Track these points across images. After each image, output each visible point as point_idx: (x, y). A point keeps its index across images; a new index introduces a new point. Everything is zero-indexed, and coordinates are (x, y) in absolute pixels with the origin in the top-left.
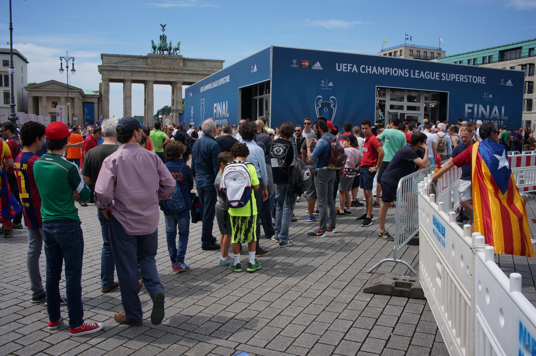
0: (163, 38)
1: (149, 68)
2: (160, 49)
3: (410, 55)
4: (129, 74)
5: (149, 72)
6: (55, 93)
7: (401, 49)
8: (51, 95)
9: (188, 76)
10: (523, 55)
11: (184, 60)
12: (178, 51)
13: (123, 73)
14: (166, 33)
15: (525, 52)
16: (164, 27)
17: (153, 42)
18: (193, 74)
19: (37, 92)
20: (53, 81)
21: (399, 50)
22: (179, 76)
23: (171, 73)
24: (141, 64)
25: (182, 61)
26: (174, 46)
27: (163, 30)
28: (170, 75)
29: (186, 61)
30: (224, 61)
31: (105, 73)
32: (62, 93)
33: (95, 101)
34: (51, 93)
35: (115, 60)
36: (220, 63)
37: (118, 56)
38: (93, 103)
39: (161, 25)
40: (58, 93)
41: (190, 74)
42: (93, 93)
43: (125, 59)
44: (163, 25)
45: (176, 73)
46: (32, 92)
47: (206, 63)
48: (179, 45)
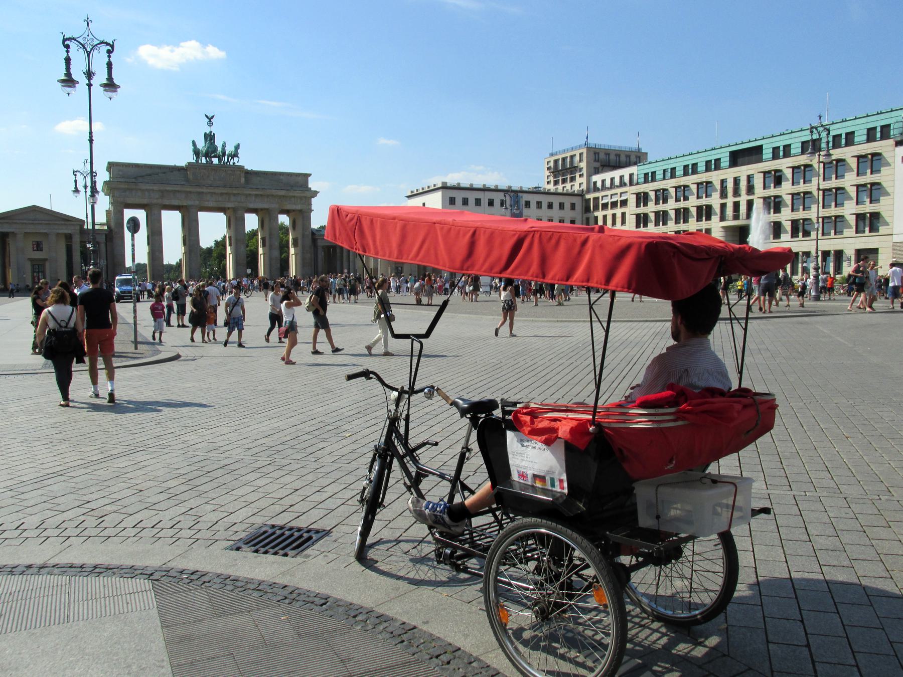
2: (207, 155)
3: (595, 161)
5: (190, 192)
7: (581, 151)
8: (31, 229)
10: (764, 157)
12: (236, 159)
14: (214, 130)
15: (767, 153)
16: (210, 119)
17: (194, 143)
20: (34, 206)
21: (577, 153)
25: (243, 175)
26: (229, 149)
27: (210, 123)
30: (310, 175)
39: (207, 116)
41: (256, 195)
44: (210, 115)
45: (234, 195)
47: (281, 177)
48: (237, 147)
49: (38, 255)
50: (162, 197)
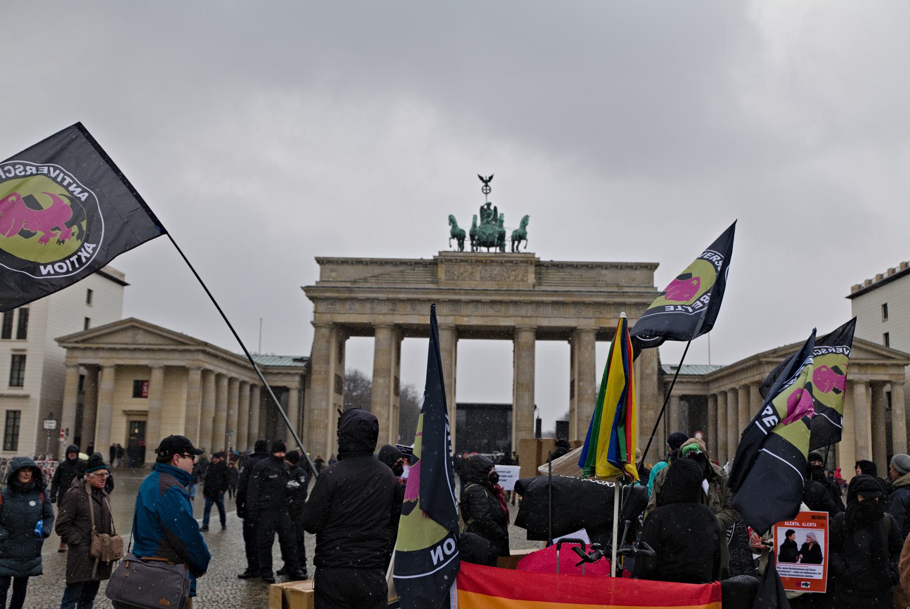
0: (488, 213)
1: (440, 291)
4: (384, 308)
6: (138, 355)
9: (549, 310)
11: (539, 264)
13: (368, 306)
14: (495, 199)
16: (486, 182)
17: (452, 221)
18: (563, 304)
19: (89, 354)
20: (132, 320)
22: (523, 311)
23: (501, 302)
24: (420, 282)
25: (532, 269)
27: (487, 189)
28: (498, 307)
29: (544, 270)
31: (323, 307)
33: (293, 383)
35: (352, 272)
36: (645, 271)
37: (359, 262)
38: (286, 390)
39: (481, 178)
40: (145, 355)
41: (555, 303)
42: (290, 363)
43: (378, 270)
44: (486, 176)
45: (515, 303)
46: (77, 353)
47: (604, 272)
48: (524, 222)
49: (139, 404)
50: (393, 311)
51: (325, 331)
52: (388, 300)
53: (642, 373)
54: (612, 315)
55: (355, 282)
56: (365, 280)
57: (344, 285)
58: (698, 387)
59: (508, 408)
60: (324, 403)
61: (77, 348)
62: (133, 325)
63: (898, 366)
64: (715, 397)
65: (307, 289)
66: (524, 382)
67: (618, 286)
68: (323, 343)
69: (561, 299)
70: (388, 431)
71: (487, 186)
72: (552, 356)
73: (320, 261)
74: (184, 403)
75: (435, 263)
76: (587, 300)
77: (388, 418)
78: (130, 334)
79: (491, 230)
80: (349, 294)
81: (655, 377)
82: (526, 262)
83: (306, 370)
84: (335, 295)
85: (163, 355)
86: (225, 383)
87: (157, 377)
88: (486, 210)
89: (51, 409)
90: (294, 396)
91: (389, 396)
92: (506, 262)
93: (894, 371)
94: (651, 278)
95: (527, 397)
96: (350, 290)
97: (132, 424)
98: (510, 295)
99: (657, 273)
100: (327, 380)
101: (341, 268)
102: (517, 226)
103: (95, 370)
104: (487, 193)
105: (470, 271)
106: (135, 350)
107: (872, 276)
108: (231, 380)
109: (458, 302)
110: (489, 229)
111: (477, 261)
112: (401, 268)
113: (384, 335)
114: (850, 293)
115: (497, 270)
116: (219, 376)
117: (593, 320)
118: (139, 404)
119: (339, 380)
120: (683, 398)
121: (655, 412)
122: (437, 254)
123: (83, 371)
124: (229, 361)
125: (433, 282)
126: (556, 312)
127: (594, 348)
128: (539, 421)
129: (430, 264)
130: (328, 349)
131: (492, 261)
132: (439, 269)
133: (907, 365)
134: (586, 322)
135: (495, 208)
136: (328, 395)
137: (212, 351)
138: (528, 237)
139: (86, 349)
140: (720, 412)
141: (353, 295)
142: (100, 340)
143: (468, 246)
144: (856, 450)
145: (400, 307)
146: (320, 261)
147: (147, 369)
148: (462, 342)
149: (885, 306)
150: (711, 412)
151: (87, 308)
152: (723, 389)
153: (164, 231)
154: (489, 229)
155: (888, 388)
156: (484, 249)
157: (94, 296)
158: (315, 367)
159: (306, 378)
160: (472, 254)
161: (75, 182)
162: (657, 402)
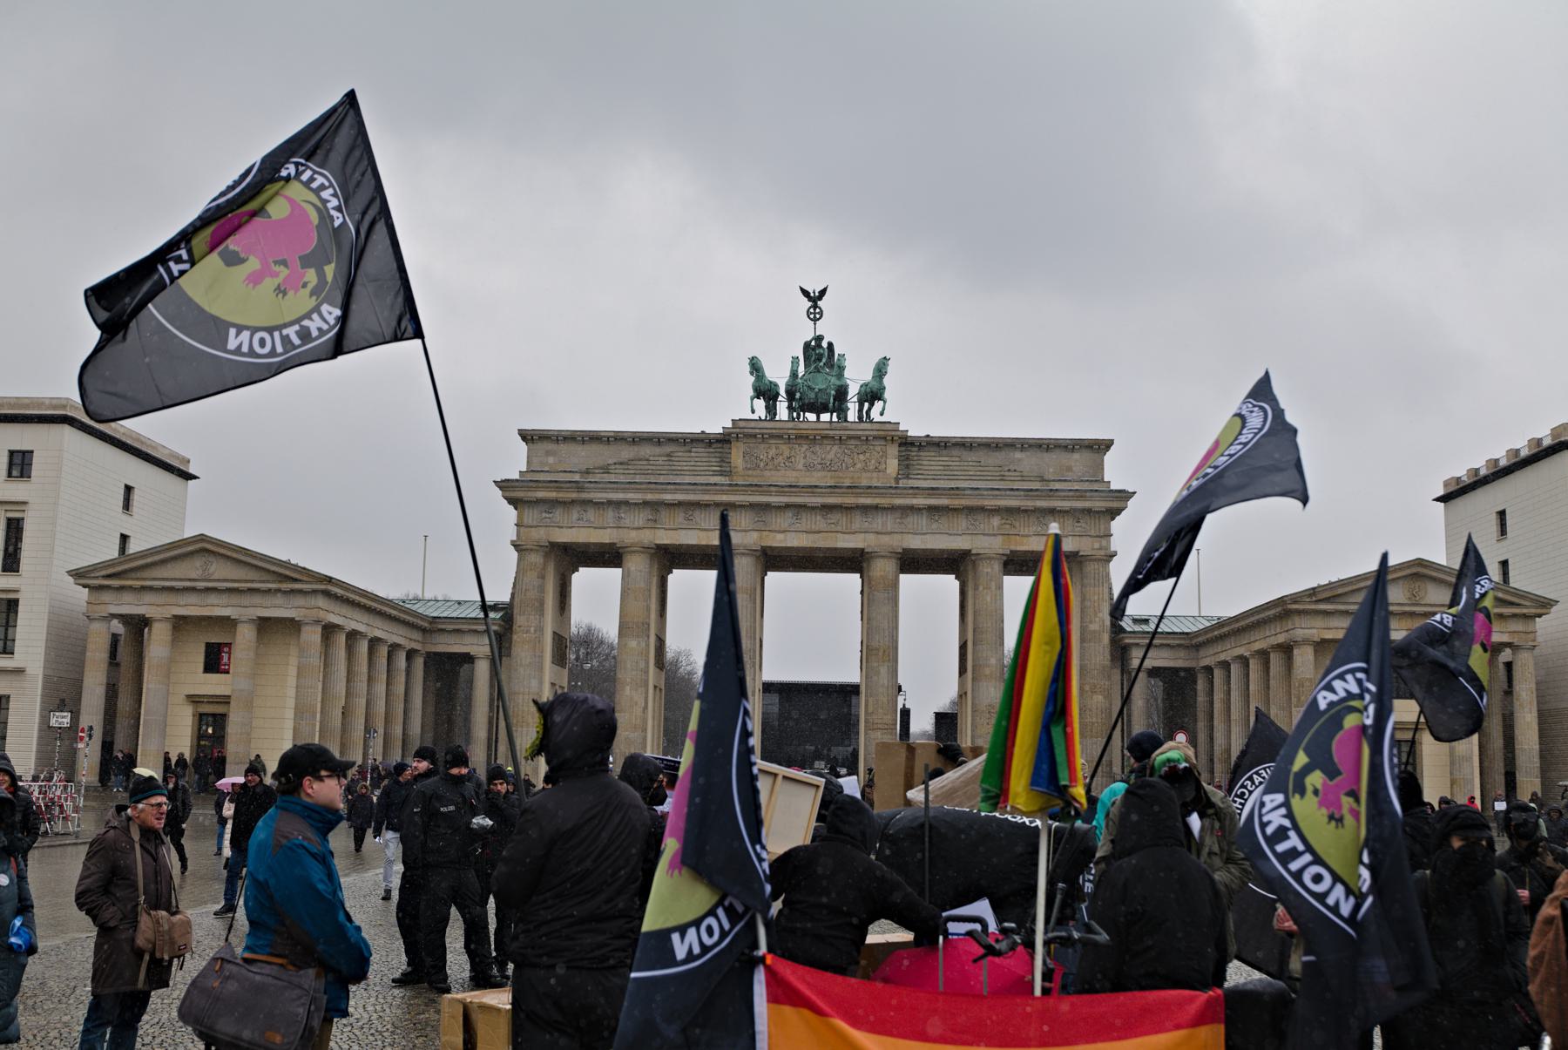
0: (818, 354)
1: (734, 487)
4: (640, 518)
6: (213, 599)
8: (191, 607)
9: (922, 522)
11: (907, 444)
13: (610, 514)
14: (829, 329)
16: (815, 298)
17: (755, 367)
19: (128, 597)
20: (202, 538)
22: (879, 522)
24: (698, 471)
25: (893, 450)
27: (815, 314)
28: (835, 517)
29: (914, 452)
31: (532, 516)
32: (246, 600)
33: (480, 647)
34: (193, 598)
37: (594, 438)
38: (468, 659)
39: (805, 293)
40: (224, 599)
41: (932, 509)
43: (627, 453)
44: (814, 288)
45: (866, 509)
46: (106, 597)
47: (1018, 455)
48: (881, 370)
49: (214, 685)
50: (653, 524)
51: (536, 559)
52: (646, 503)
53: (1083, 629)
54: (1033, 529)
55: (588, 472)
56: (606, 469)
57: (568, 477)
58: (1182, 653)
59: (853, 690)
60: (534, 683)
61: (108, 587)
62: (204, 547)
63: (1525, 616)
64: (1209, 670)
65: (504, 485)
66: (880, 646)
67: (1043, 480)
68: (531, 578)
69: (944, 502)
70: (645, 730)
71: (815, 306)
72: (929, 601)
73: (526, 436)
74: (292, 681)
75: (723, 440)
76: (989, 503)
77: (646, 707)
78: (198, 562)
79: (824, 383)
80: (578, 493)
81: (1106, 638)
82: (885, 438)
83: (500, 624)
84: (553, 495)
85: (257, 599)
86: (363, 647)
87: (245, 636)
88: (814, 349)
89: (63, 695)
90: (482, 669)
91: (647, 672)
92: (850, 438)
93: (1517, 626)
94: (1100, 467)
95: (883, 670)
96: (578, 486)
97: (201, 718)
98: (858, 495)
99: (1109, 458)
100: (539, 641)
101: (564, 448)
102: (868, 376)
103: (138, 626)
104: (815, 320)
105: (787, 453)
106: (208, 590)
107: (1479, 461)
108: (374, 642)
109: (765, 507)
110: (818, 383)
111: (798, 437)
112: (668, 449)
113: (638, 564)
114: (1441, 492)
115: (832, 452)
116: (353, 636)
117: (1000, 538)
118: (214, 685)
119: (561, 644)
120: (1154, 672)
121: (1108, 697)
122: (730, 425)
123: (117, 627)
124: (369, 610)
125: (722, 473)
126: (935, 526)
127: (1000, 587)
128: (906, 713)
129: (718, 441)
130: (542, 589)
131: (825, 437)
132: (734, 451)
133: (1540, 616)
134: (986, 541)
135: (830, 345)
136: (541, 668)
137: (339, 591)
138: (886, 395)
139: (122, 588)
140: (1218, 696)
141: (584, 496)
142: (146, 574)
143: (782, 411)
144: (1452, 763)
145: (664, 515)
146: (526, 436)
147: (228, 623)
148: (772, 578)
149: (1502, 514)
150: (1201, 698)
151: (124, 517)
152: (1222, 657)
153: (418, 334)
154: (818, 383)
155: (1506, 655)
156: (811, 417)
157: (136, 497)
158: (520, 620)
159: (502, 640)
160: (791, 425)
161: (331, 185)
162: (1109, 678)
